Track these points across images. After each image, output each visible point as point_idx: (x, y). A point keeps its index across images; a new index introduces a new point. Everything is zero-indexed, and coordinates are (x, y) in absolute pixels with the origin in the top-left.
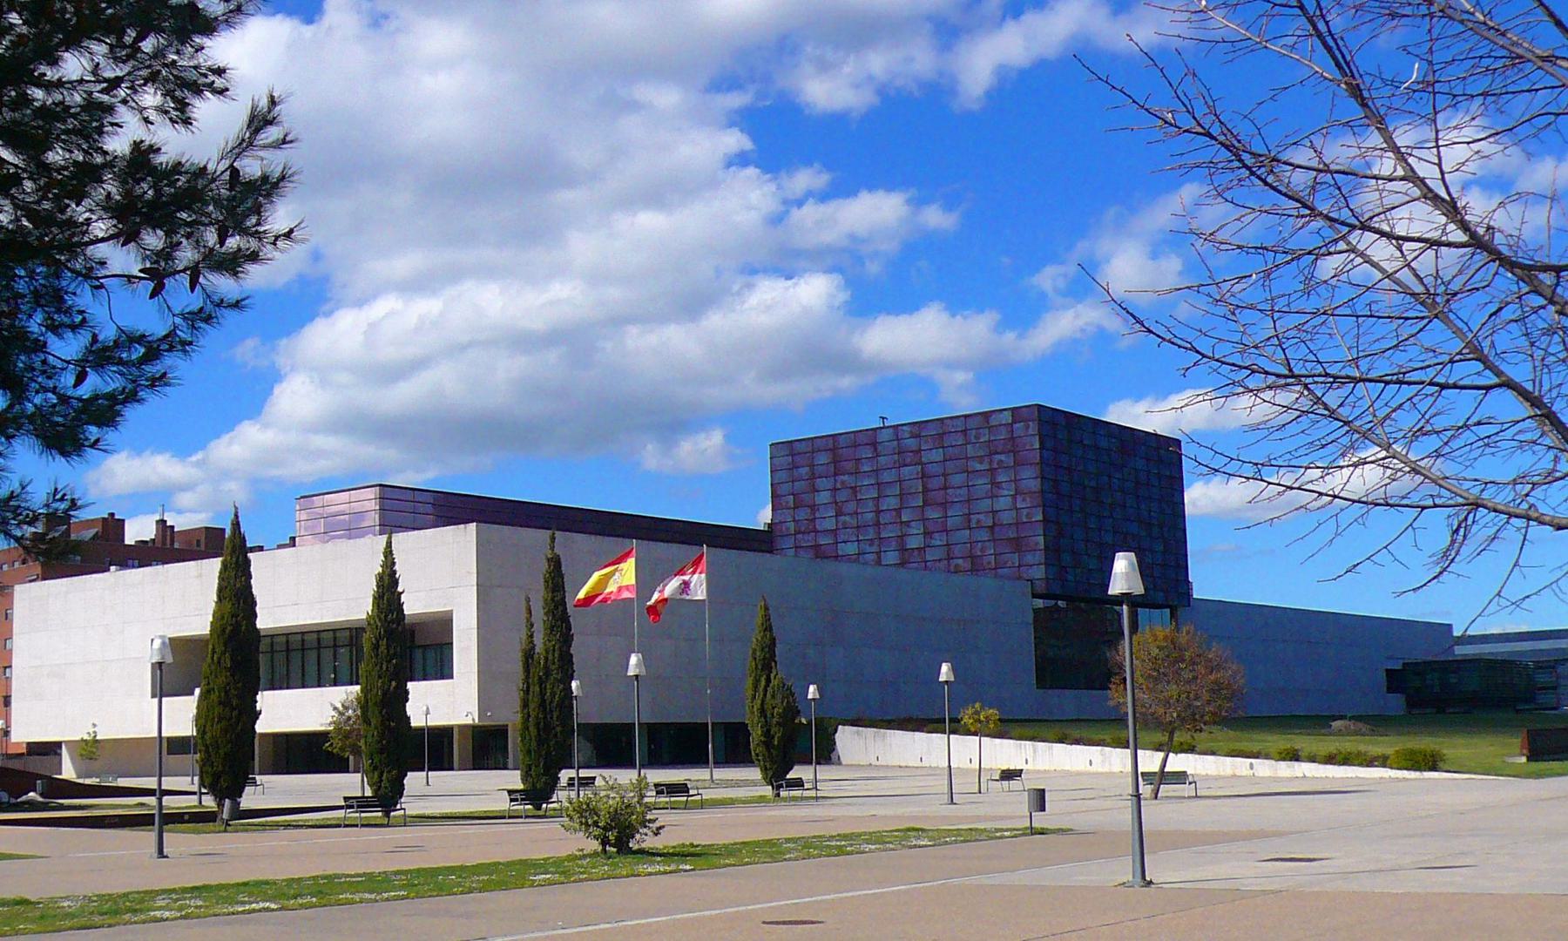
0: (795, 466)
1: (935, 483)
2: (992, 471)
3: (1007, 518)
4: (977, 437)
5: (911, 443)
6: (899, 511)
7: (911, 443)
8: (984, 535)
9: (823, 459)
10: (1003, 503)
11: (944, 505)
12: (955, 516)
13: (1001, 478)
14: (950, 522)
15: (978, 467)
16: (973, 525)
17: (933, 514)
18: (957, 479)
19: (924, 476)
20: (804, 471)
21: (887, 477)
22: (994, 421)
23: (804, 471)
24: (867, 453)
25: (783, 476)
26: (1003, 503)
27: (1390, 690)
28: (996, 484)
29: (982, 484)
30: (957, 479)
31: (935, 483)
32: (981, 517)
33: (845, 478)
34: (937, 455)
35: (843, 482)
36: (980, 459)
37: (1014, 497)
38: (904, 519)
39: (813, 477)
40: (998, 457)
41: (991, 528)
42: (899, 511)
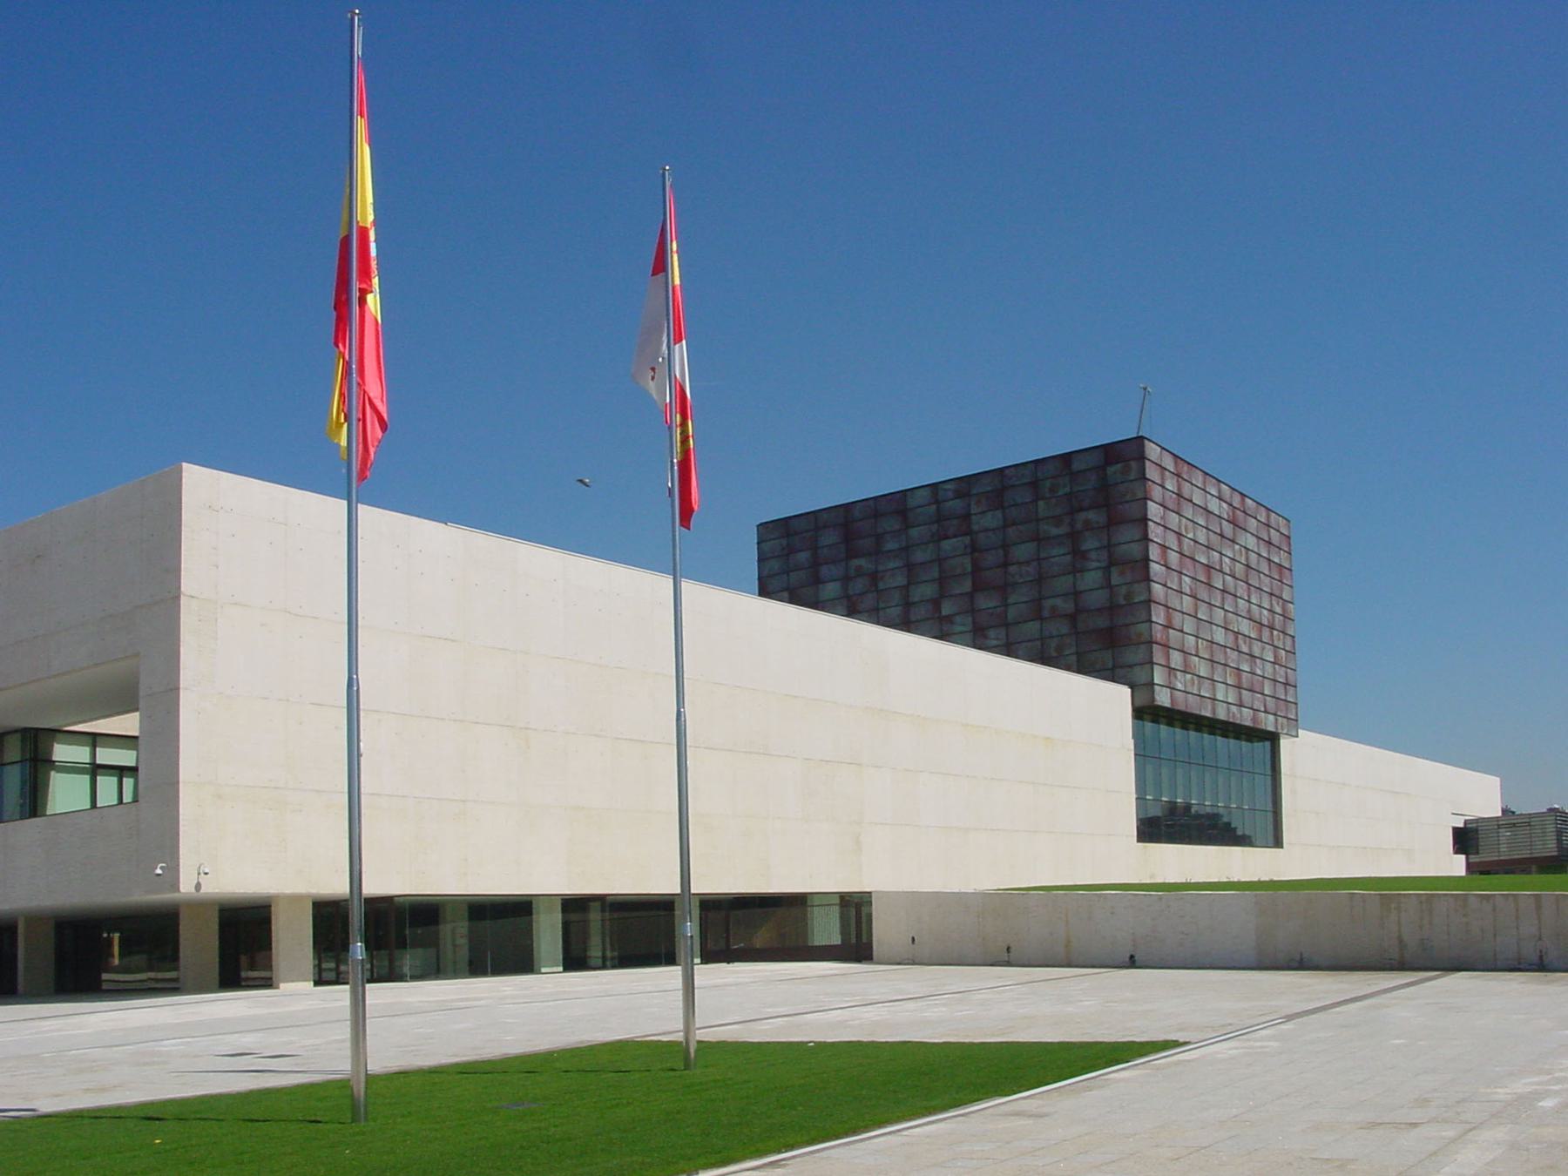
0: (790, 551)
1: (991, 558)
2: (1074, 536)
3: (1097, 599)
4: (1052, 490)
5: (955, 505)
6: (936, 603)
7: (955, 505)
8: (1063, 628)
9: (829, 538)
10: (1091, 578)
11: (1004, 589)
12: (1019, 599)
13: (1090, 543)
14: (1012, 613)
15: (1055, 531)
16: (1046, 613)
17: (986, 602)
18: (1023, 551)
19: (974, 548)
20: (803, 557)
21: (919, 556)
22: (1077, 465)
23: (803, 557)
24: (890, 524)
25: (775, 565)
26: (1091, 578)
27: (1456, 852)
28: (1079, 554)
29: (1059, 555)
30: (1023, 551)
31: (991, 558)
32: (1058, 602)
33: (861, 562)
34: (991, 520)
35: (859, 568)
36: (1057, 520)
37: (1107, 570)
38: (944, 613)
39: (816, 564)
40: (1082, 516)
41: (1073, 618)
42: (936, 603)
